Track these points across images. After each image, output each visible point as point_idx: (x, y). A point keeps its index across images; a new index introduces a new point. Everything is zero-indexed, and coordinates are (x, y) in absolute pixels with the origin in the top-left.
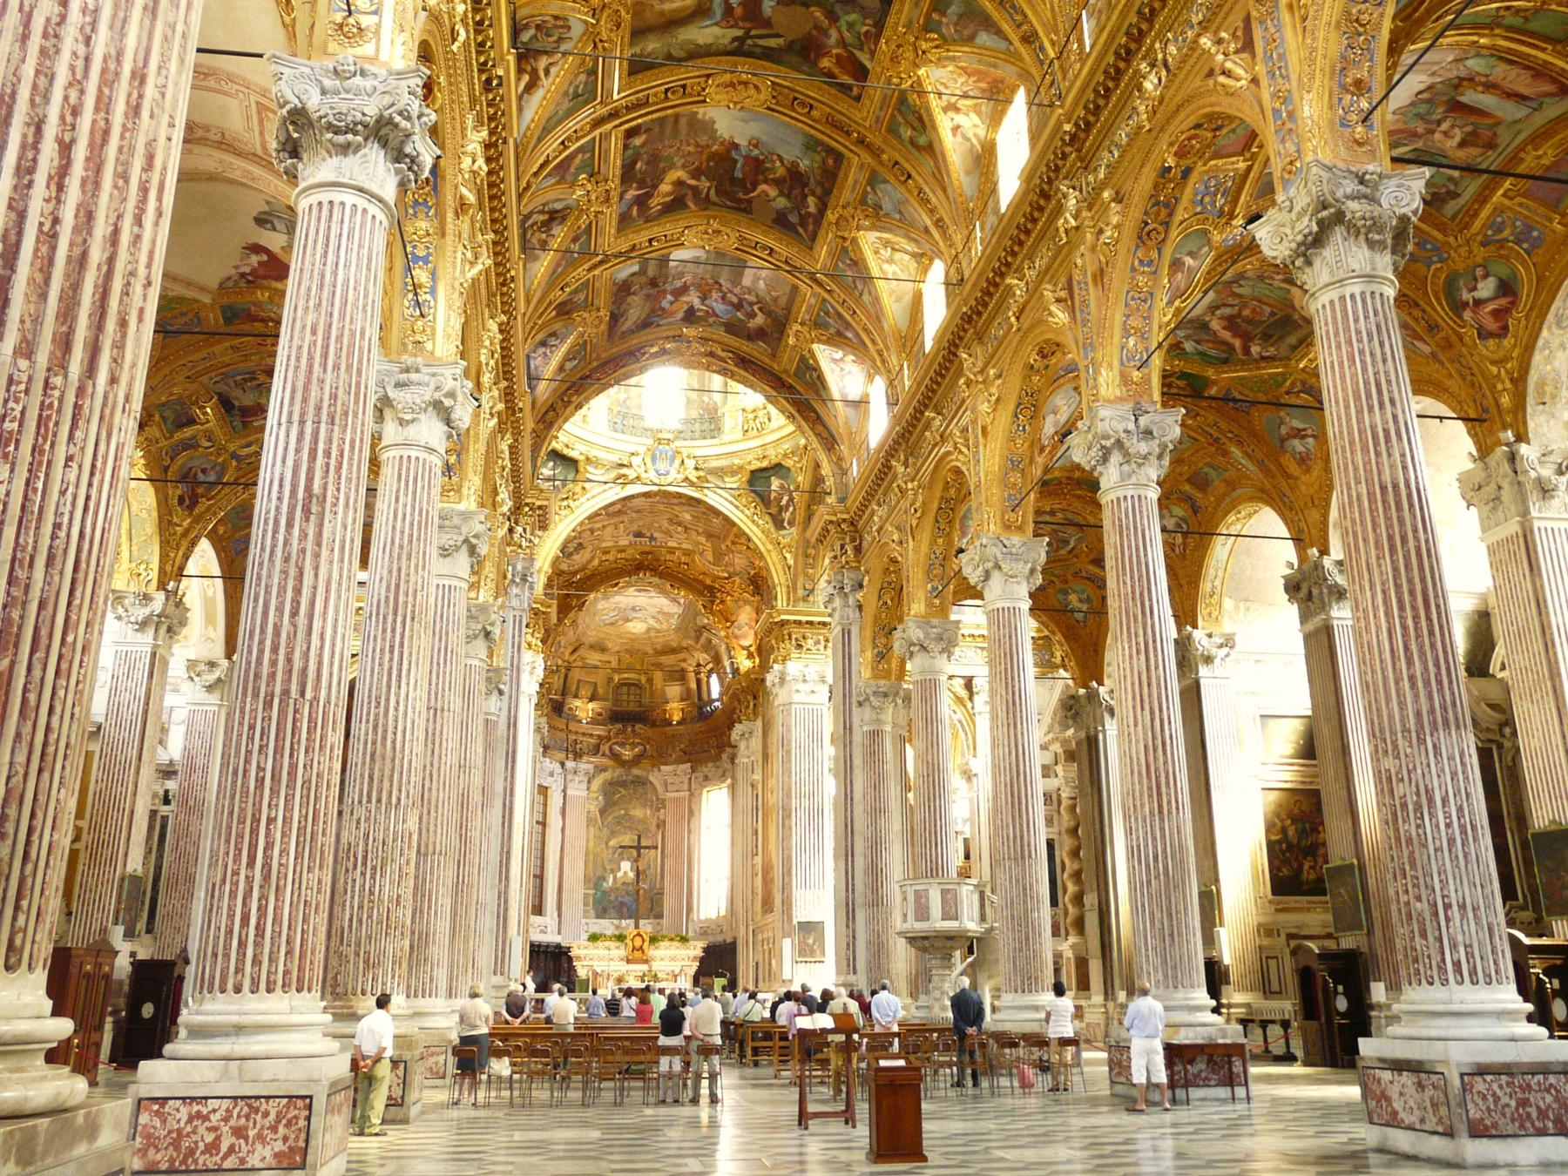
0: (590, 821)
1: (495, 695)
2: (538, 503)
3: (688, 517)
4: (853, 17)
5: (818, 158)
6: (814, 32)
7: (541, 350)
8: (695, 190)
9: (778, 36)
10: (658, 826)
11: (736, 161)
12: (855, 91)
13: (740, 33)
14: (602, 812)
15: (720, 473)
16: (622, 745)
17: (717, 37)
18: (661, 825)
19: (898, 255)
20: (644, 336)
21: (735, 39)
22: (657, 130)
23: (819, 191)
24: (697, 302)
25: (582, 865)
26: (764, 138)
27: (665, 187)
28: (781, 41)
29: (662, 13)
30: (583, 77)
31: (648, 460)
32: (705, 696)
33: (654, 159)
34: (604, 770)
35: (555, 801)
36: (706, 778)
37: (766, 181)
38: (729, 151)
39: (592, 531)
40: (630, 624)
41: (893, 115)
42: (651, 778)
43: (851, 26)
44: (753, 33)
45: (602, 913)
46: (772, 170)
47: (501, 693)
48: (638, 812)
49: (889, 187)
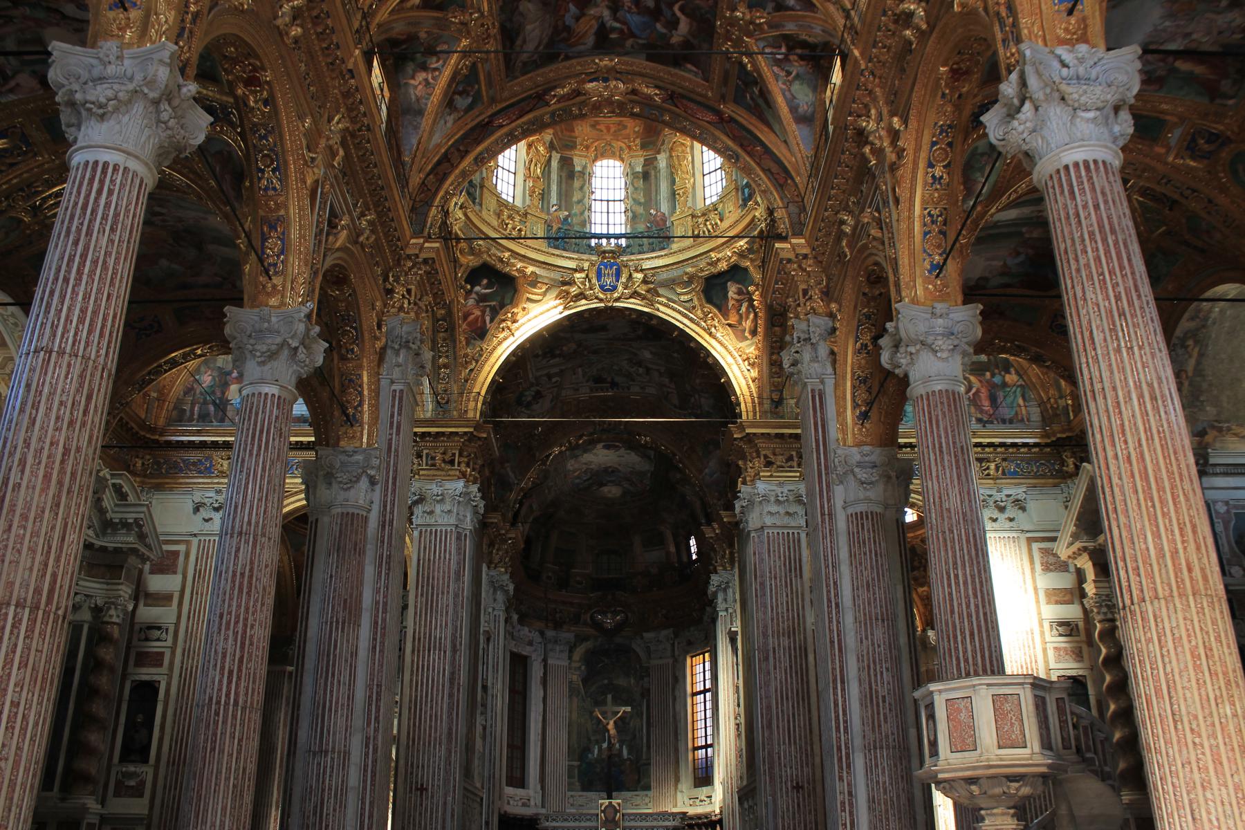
0: (573, 691)
1: (364, 483)
2: (423, 256)
3: (647, 355)
7: (421, 76)
10: (643, 695)
14: (585, 681)
15: (670, 284)
16: (604, 613)
18: (646, 693)
20: (550, 72)
24: (606, 13)
25: (565, 736)
31: (593, 276)
32: (685, 559)
34: (586, 639)
35: (536, 671)
36: (690, 643)
39: (549, 377)
40: (605, 489)
42: (634, 646)
45: (587, 787)
47: (373, 482)
48: (622, 682)
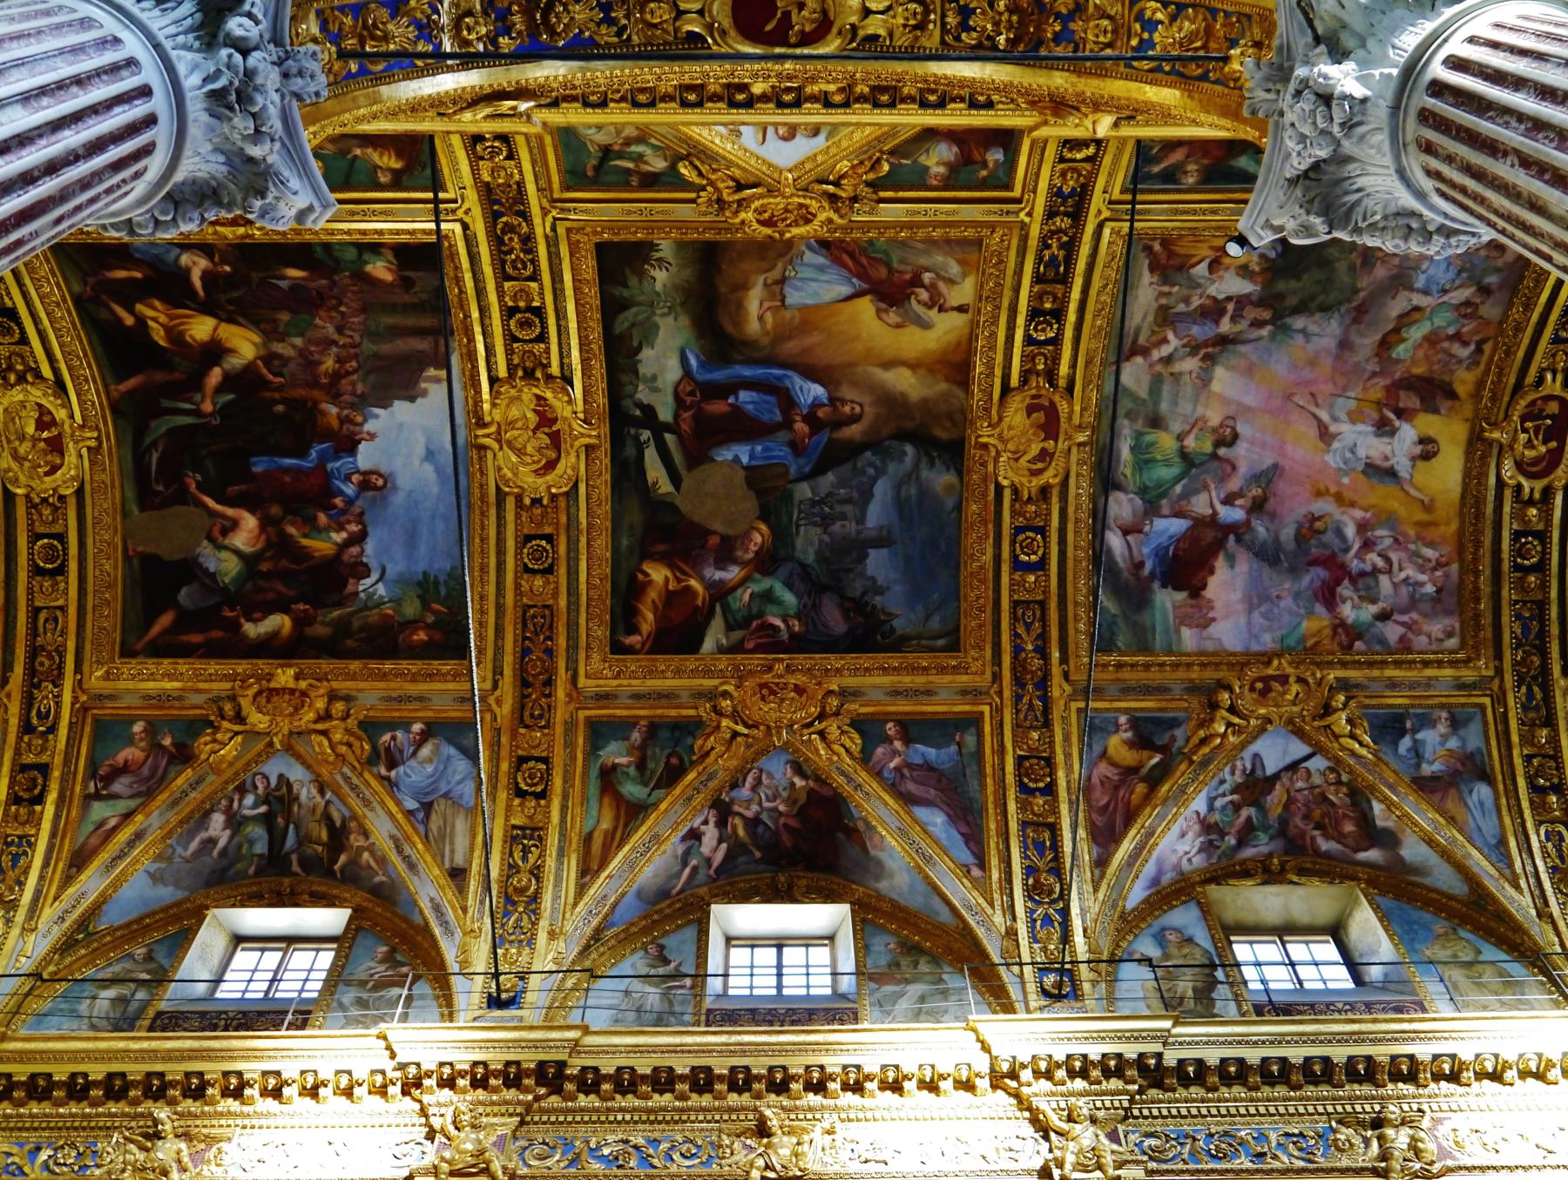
4: (789, 598)
5: (411, 609)
6: (714, 541)
8: (195, 382)
9: (676, 480)
11: (302, 453)
12: (634, 640)
13: (665, 414)
17: (654, 378)
19: (258, 832)
21: (649, 411)
22: (407, 298)
23: (320, 630)
26: (398, 499)
27: (201, 328)
28: (665, 486)
29: (744, 286)
30: (658, 164)
33: (304, 302)
37: (264, 523)
38: (327, 435)
41: (631, 723)
43: (768, 597)
44: (668, 437)
46: (313, 528)
49: (461, 765)
